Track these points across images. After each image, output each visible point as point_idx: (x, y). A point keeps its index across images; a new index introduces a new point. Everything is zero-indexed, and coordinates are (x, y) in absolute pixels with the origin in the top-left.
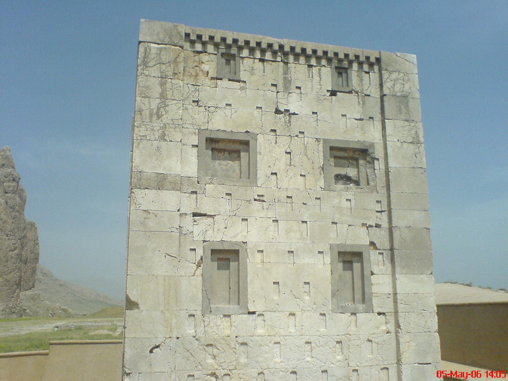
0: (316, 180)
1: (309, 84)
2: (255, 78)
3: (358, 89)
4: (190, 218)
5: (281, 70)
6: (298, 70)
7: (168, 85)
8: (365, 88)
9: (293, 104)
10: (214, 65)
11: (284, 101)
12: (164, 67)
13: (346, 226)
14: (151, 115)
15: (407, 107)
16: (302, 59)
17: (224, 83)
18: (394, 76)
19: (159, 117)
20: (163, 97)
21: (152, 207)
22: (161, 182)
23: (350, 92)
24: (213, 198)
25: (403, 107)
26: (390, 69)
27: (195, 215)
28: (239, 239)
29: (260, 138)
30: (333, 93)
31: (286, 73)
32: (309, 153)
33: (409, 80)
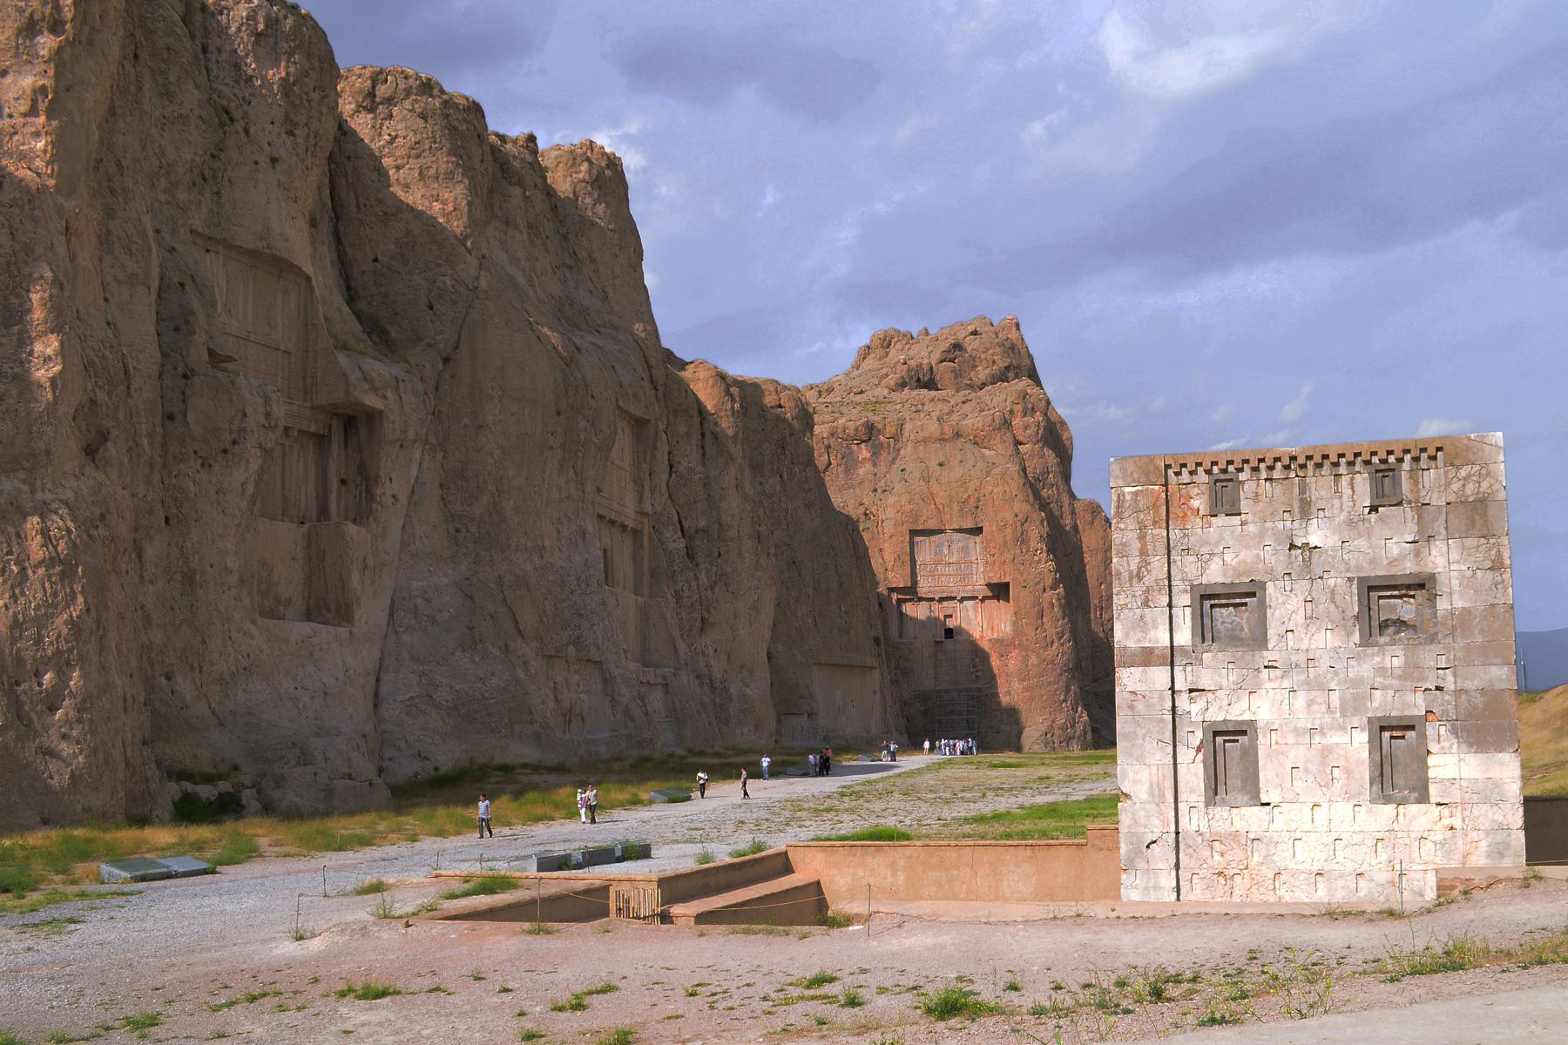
0: (1349, 634)
1: (1337, 502)
2: (1260, 506)
3: (1411, 497)
4: (1185, 696)
5: (1296, 490)
6: (1319, 485)
7: (1149, 538)
8: (1423, 493)
9: (1317, 534)
10: (1205, 498)
11: (1301, 533)
12: (1142, 516)
13: (1391, 692)
14: (1131, 579)
16: (1326, 470)
17: (1221, 520)
18: (1463, 473)
19: (1140, 578)
20: (1143, 552)
21: (1139, 688)
22: (1147, 658)
23: (1400, 504)
24: (1213, 670)
25: (1477, 517)
26: (1456, 462)
27: (1191, 691)
28: (1247, 717)
29: (1270, 586)
30: (1374, 509)
31: (1302, 491)
32: (1338, 599)
33: (1488, 474)
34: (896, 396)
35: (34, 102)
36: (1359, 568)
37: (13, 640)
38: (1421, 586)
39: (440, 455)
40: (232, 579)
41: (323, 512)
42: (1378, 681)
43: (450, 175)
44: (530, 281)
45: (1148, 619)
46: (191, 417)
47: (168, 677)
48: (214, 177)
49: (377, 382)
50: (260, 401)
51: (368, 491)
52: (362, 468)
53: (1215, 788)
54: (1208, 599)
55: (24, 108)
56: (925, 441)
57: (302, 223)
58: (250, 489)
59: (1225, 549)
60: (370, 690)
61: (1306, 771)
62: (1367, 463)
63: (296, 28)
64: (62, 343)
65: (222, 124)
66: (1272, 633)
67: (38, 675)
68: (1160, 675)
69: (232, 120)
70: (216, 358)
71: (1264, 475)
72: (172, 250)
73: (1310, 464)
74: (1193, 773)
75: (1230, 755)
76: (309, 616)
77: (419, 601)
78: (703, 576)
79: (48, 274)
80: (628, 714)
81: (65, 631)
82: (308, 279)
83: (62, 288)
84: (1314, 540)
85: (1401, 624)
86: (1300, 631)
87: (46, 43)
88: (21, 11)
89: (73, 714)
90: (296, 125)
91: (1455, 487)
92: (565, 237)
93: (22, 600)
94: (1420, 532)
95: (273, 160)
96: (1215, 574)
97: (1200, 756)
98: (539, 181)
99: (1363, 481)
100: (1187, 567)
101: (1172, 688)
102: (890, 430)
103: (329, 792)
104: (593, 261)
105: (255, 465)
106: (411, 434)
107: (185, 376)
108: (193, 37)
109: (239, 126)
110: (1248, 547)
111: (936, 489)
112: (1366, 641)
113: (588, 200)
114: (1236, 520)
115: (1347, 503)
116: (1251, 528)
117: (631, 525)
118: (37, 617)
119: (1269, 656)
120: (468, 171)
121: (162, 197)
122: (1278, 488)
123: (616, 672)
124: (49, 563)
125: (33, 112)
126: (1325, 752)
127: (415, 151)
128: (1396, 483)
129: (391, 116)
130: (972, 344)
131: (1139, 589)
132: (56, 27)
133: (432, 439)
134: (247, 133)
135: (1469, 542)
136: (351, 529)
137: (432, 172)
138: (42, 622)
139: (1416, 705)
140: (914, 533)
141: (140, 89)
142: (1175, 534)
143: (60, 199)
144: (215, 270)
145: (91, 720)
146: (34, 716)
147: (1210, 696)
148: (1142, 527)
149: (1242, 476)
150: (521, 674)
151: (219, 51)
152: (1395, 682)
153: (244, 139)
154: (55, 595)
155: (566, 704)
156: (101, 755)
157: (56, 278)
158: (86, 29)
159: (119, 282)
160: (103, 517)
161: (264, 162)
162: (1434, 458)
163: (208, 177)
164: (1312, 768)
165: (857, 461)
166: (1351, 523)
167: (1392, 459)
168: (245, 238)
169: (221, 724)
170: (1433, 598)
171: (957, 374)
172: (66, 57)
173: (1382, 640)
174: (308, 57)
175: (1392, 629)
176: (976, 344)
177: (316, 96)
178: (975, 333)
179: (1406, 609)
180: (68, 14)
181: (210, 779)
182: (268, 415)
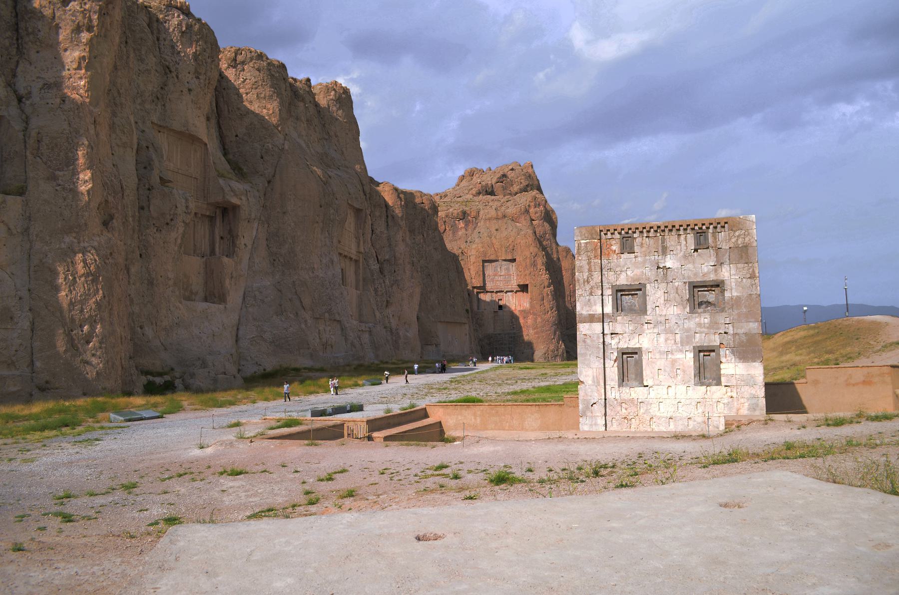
0: (685, 308)
2: (644, 249)
4: (609, 336)
5: (660, 242)
6: (671, 240)
9: (670, 262)
15: (747, 253)
16: (674, 232)
17: (626, 255)
18: (737, 233)
19: (588, 282)
20: (590, 270)
21: (588, 332)
22: (591, 319)
23: (708, 248)
24: (622, 324)
28: (637, 346)
29: (648, 286)
30: (696, 250)
31: (663, 242)
34: (476, 199)
35: (80, 63)
36: (689, 277)
37: (70, 311)
38: (718, 286)
39: (266, 226)
40: (171, 283)
41: (213, 252)
42: (698, 329)
43: (271, 97)
44: (308, 146)
45: (592, 301)
46: (152, 208)
47: (141, 328)
48: (162, 98)
49: (237, 192)
50: (184, 201)
51: (233, 242)
52: (230, 231)
53: (623, 379)
54: (620, 292)
55: (75, 66)
56: (489, 219)
57: (203, 119)
58: (179, 241)
59: (628, 269)
60: (234, 333)
61: (665, 371)
62: (693, 229)
63: (200, 29)
64: (92, 174)
65: (166, 74)
66: (649, 307)
67: (81, 326)
68: (597, 327)
69: (171, 72)
70: (163, 181)
71: (645, 235)
72: (143, 131)
73: (667, 230)
74: (613, 372)
75: (630, 364)
76: (206, 300)
77: (257, 293)
78: (387, 281)
79: (86, 143)
80: (353, 345)
81: (94, 306)
82: (206, 144)
83: (92, 148)
84: (668, 265)
85: (708, 303)
86: (662, 307)
87: (85, 36)
88: (74, 21)
89: (97, 345)
90: (200, 74)
91: (733, 240)
92: (324, 125)
93: (74, 292)
94: (717, 261)
95: (190, 90)
96: (623, 281)
97: (616, 364)
98: (312, 100)
99: (691, 237)
100: (610, 277)
101: (603, 333)
102: (473, 214)
103: (215, 380)
104: (337, 136)
105: (181, 230)
106: (253, 216)
107: (149, 189)
108: (152, 33)
109: (174, 74)
110: (637, 268)
111: (494, 241)
112: (692, 311)
113: (334, 109)
114: (632, 255)
115: (684, 248)
116: (639, 259)
117: (354, 257)
118: (81, 300)
119: (647, 318)
120: (279, 95)
121: (138, 107)
122: (652, 241)
123: (347, 325)
124: (86, 275)
125: (79, 68)
126: (674, 362)
127: (255, 86)
128: (706, 239)
129: (244, 70)
130: (511, 175)
131: (588, 287)
132: (89, 29)
133: (263, 218)
134: (177, 77)
135: (740, 265)
136: (225, 260)
137: (262, 96)
138: (83, 302)
139: (715, 340)
140: (484, 261)
141: (128, 57)
142: (604, 262)
143: (92, 108)
144: (163, 140)
145: (106, 348)
146: (80, 346)
147: (621, 336)
148: (589, 259)
149: (635, 235)
150: (303, 326)
151: (165, 40)
152: (706, 330)
153: (176, 80)
154: (89, 290)
155: (324, 340)
156: (110, 363)
157: (90, 144)
158: (103, 30)
159: (118, 146)
160: (111, 254)
161: (185, 91)
162: (723, 227)
163: (160, 98)
164: (668, 369)
165: (458, 228)
166: (685, 257)
167: (704, 227)
168: (177, 126)
169: (166, 349)
170: (723, 291)
171: (504, 188)
172: (94, 42)
173: (700, 311)
174: (206, 43)
175: (704, 306)
176: (513, 175)
177: (209, 60)
178: (512, 169)
179: (711, 296)
180: (95, 23)
181: (160, 374)
182: (187, 207)
